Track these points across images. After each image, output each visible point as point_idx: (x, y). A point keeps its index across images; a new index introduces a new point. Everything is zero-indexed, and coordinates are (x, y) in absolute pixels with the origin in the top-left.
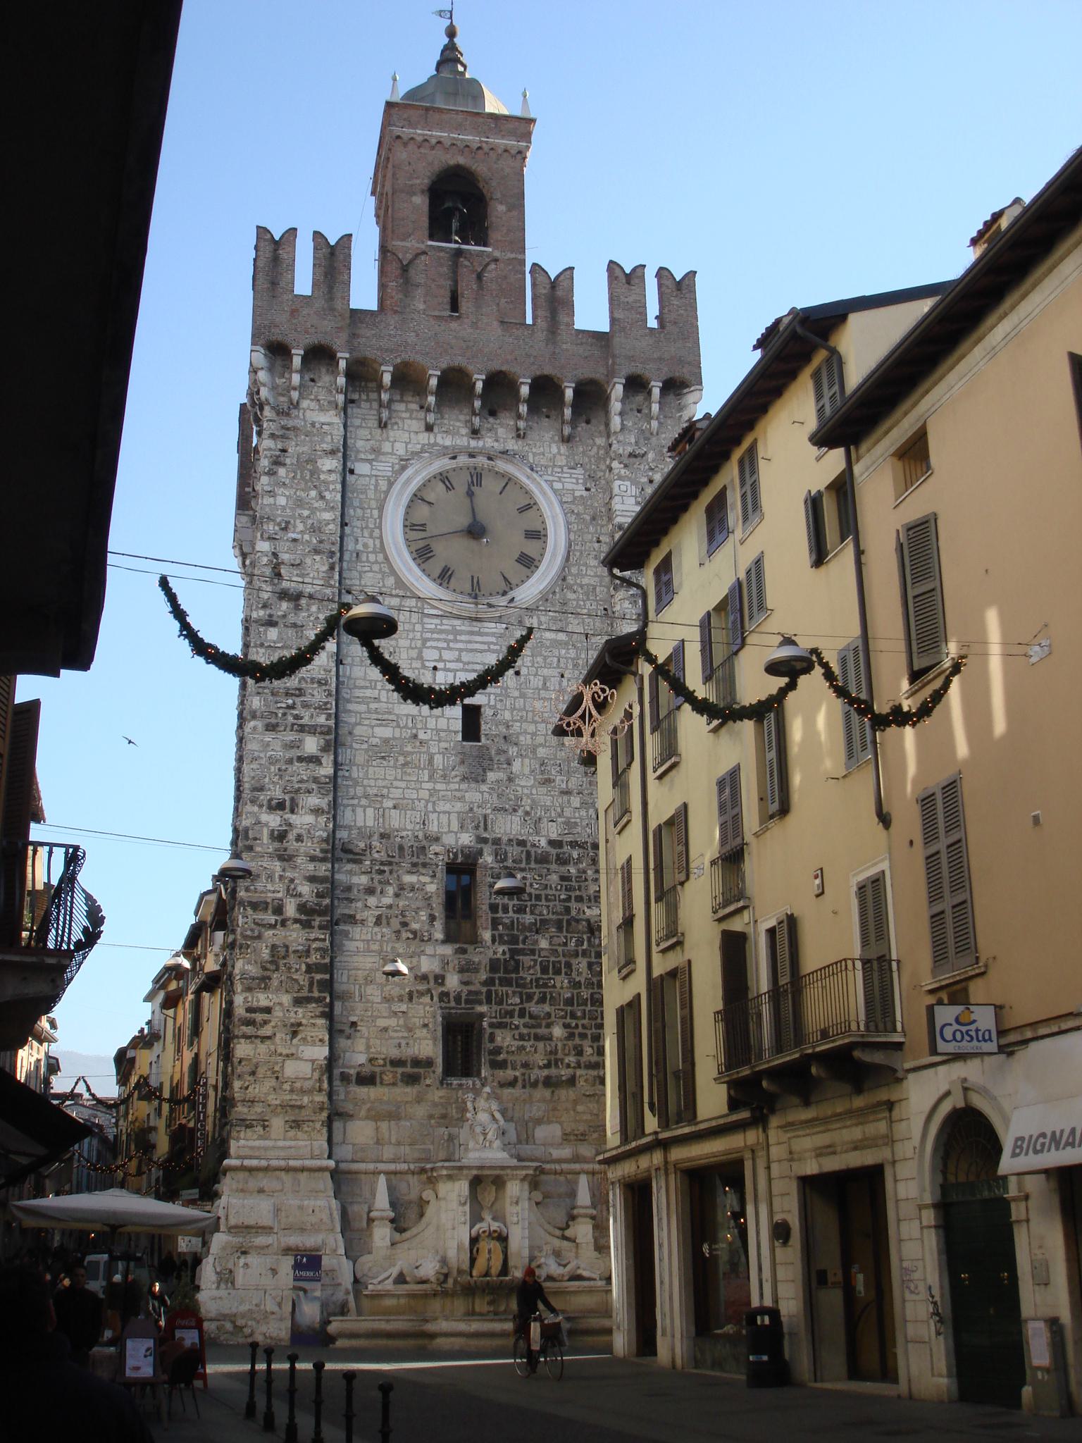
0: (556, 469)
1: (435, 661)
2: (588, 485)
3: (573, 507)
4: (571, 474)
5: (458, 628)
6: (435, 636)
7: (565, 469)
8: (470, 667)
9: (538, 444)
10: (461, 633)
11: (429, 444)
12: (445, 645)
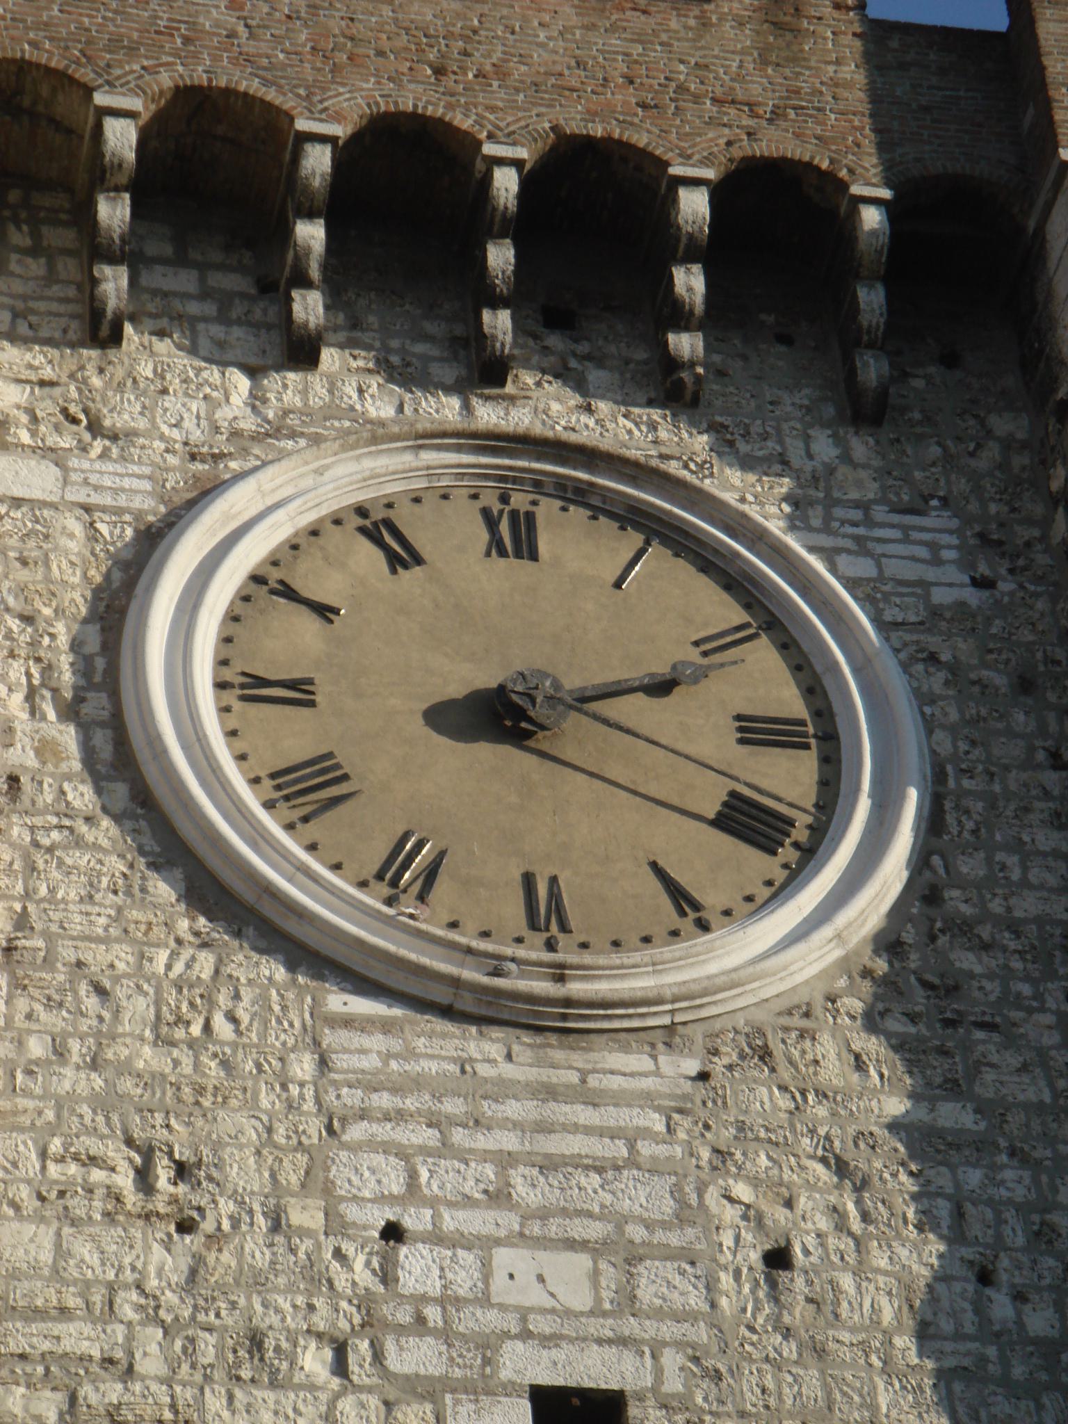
0: (838, 512)
1: (391, 1199)
2: (983, 569)
3: (933, 642)
4: (905, 529)
5: (484, 1070)
6: (384, 1100)
7: (879, 513)
8: (554, 1228)
9: (756, 427)
10: (502, 1090)
11: (306, 412)
12: (428, 1136)
